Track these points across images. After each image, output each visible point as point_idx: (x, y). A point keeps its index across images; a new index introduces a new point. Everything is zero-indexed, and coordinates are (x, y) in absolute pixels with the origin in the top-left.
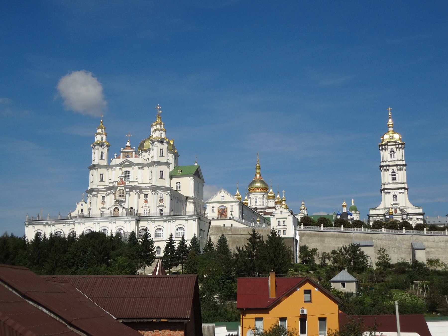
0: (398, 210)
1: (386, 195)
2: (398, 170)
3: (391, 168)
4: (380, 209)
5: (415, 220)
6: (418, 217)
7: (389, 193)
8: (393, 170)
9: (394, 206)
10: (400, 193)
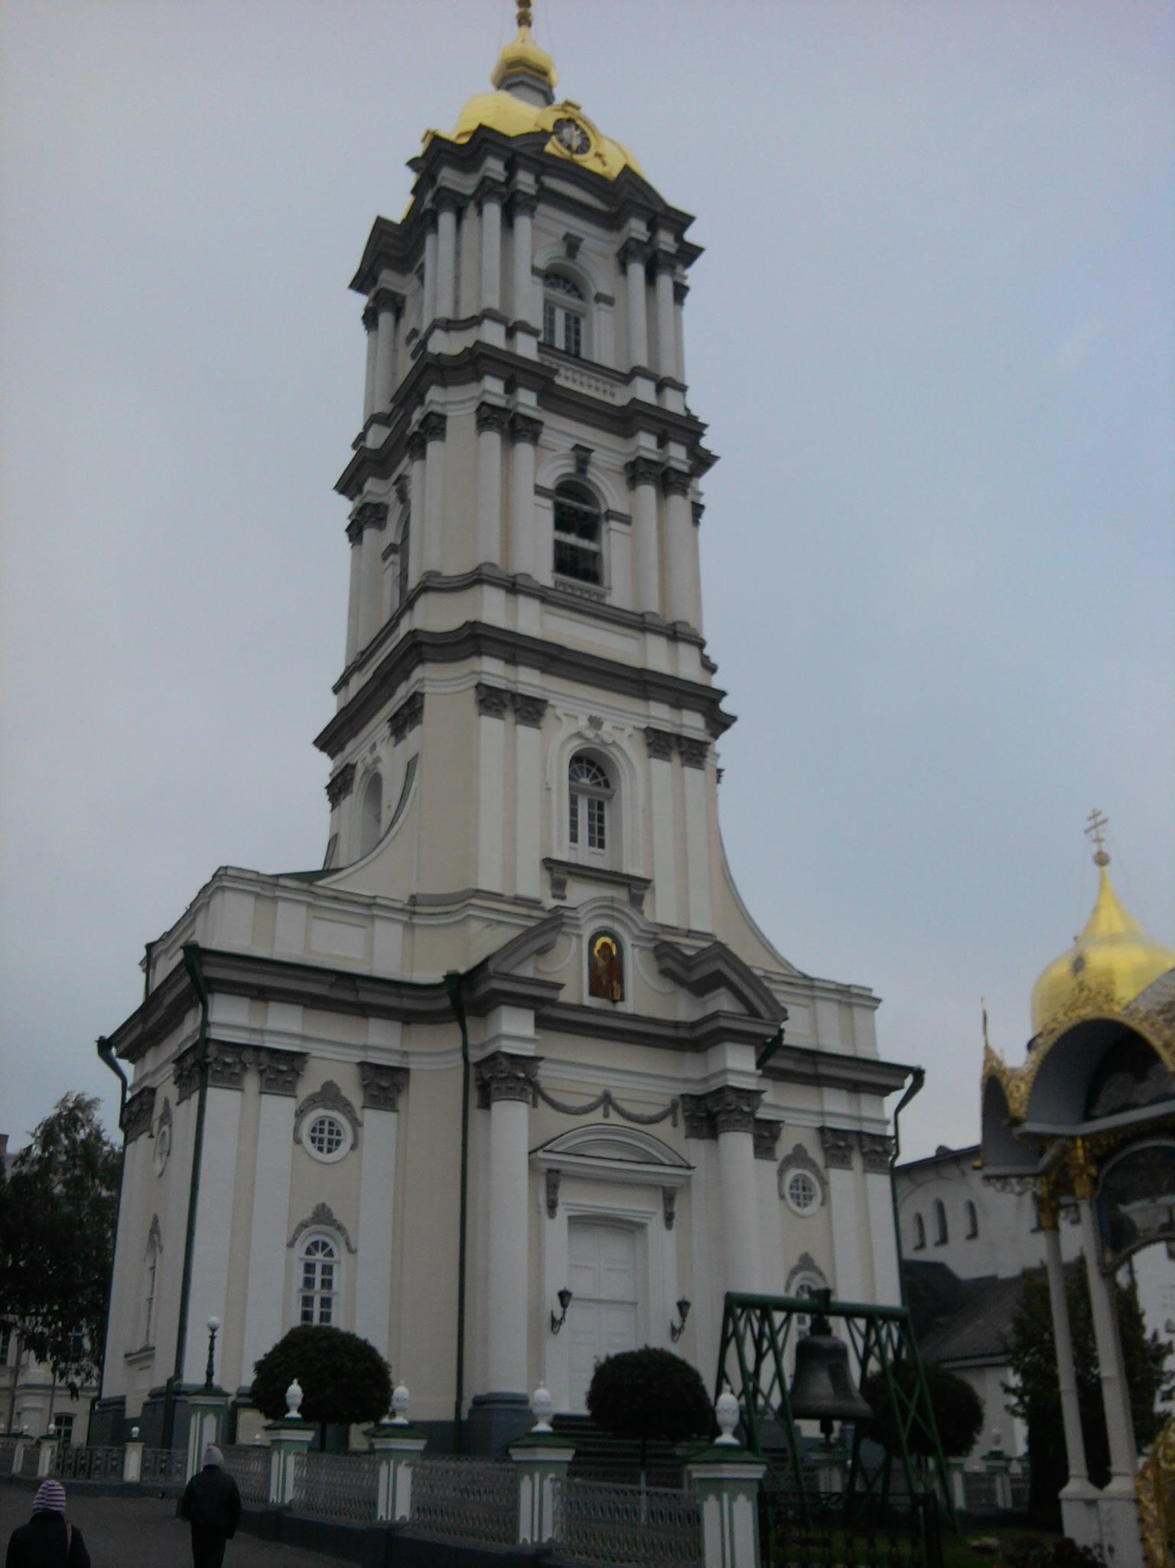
0: (637, 967)
1: (494, 729)
2: (636, 472)
3: (562, 434)
4: (370, 907)
5: (799, 1157)
6: (838, 1108)
7: (531, 710)
8: (582, 455)
9: (579, 893)
10: (660, 743)
